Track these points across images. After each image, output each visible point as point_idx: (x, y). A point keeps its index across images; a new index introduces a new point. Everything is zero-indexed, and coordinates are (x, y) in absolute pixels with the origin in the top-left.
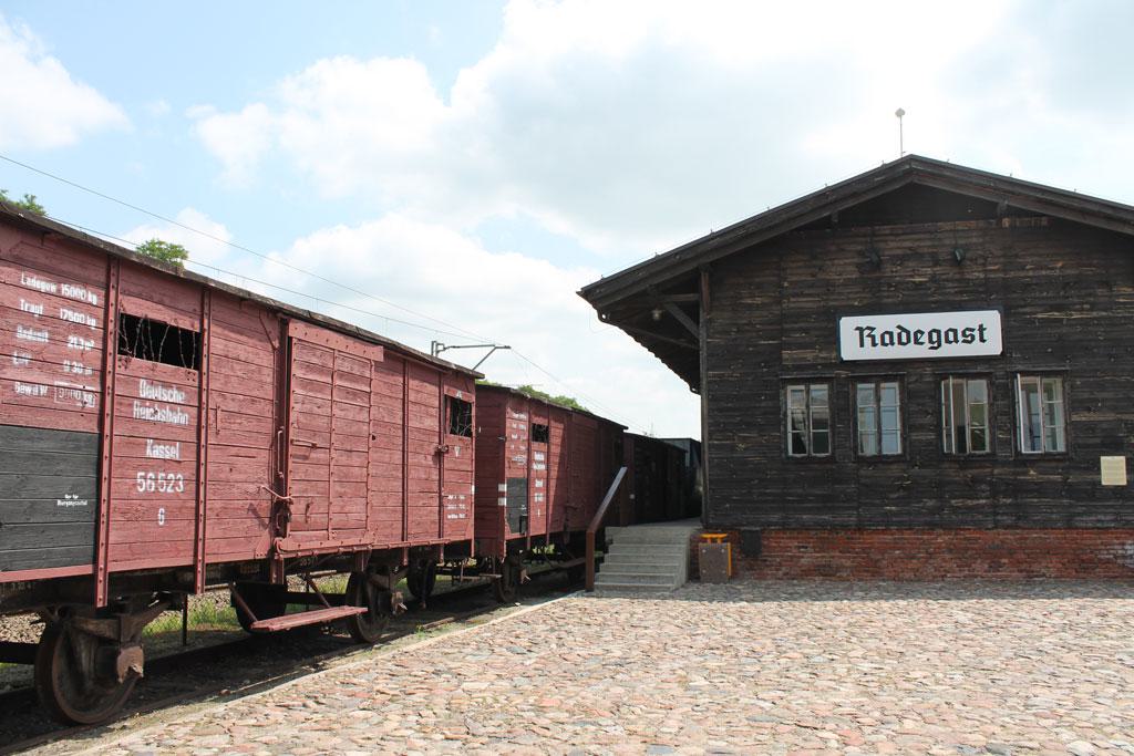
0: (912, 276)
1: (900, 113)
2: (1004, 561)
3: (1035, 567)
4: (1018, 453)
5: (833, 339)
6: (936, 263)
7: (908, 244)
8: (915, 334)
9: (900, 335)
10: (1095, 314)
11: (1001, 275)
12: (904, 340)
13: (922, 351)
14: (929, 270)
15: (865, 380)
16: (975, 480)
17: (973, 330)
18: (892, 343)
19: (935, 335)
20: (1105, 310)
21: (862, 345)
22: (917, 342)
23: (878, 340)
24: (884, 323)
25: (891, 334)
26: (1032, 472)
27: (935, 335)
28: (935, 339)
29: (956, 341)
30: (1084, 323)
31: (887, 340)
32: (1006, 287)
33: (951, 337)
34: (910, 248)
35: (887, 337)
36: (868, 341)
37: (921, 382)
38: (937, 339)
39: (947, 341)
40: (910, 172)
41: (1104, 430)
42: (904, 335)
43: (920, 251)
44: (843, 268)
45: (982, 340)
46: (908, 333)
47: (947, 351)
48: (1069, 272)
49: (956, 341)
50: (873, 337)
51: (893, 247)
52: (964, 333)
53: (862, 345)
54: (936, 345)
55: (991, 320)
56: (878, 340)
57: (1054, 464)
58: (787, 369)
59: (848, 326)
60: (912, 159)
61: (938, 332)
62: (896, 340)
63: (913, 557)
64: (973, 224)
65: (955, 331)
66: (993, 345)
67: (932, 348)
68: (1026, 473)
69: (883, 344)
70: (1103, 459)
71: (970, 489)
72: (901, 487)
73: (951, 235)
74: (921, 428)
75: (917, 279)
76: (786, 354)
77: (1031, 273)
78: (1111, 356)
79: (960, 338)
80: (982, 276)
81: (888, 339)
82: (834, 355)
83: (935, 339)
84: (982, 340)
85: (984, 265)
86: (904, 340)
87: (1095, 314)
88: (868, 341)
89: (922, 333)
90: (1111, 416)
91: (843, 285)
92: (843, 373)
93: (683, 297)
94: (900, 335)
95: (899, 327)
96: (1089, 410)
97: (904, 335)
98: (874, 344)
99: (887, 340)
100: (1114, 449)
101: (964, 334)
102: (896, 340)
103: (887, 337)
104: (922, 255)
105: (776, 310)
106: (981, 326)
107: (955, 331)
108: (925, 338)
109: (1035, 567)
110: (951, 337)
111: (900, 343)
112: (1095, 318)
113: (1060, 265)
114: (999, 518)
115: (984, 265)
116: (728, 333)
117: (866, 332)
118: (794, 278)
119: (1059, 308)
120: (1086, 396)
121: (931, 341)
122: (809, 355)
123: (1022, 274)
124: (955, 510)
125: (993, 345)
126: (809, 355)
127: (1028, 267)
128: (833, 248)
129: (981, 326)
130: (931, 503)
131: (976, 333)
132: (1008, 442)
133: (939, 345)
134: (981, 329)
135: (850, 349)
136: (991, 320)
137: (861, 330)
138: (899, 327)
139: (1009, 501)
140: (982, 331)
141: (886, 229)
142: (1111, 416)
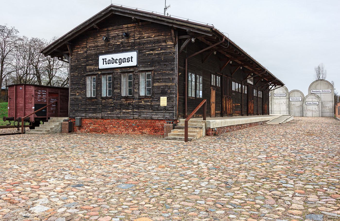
0: (117, 42)
2: (136, 129)
3: (144, 131)
4: (139, 96)
5: (97, 64)
6: (123, 38)
7: (117, 32)
8: (116, 60)
9: (112, 60)
10: (161, 51)
11: (138, 40)
12: (113, 62)
14: (121, 40)
15: (104, 74)
16: (129, 104)
17: (129, 58)
18: (110, 63)
19: (120, 60)
20: (164, 50)
21: (103, 64)
22: (116, 63)
23: (107, 63)
24: (108, 57)
25: (110, 60)
26: (143, 102)
27: (120, 60)
28: (120, 61)
29: (125, 62)
30: (158, 54)
31: (109, 63)
32: (139, 44)
33: (124, 59)
34: (116, 34)
36: (105, 62)
37: (114, 74)
38: (121, 61)
39: (123, 62)
40: (112, 10)
41: (162, 89)
42: (113, 60)
43: (119, 34)
44: (101, 41)
45: (132, 61)
46: (114, 60)
47: (124, 65)
48: (156, 38)
49: (125, 62)
50: (106, 61)
51: (113, 34)
52: (127, 59)
53: (103, 64)
54: (120, 63)
55: (134, 54)
56: (107, 63)
57: (149, 99)
58: (87, 72)
59: (101, 58)
60: (111, 6)
61: (121, 59)
62: (111, 62)
63: (115, 127)
64: (132, 25)
66: (134, 63)
67: (119, 64)
68: (141, 102)
69: (108, 64)
70: (161, 97)
71: (127, 107)
72: (111, 106)
73: (126, 29)
74: (117, 88)
75: (118, 43)
76: (87, 67)
77: (146, 39)
78: (165, 65)
79: (126, 61)
80: (133, 41)
82: (98, 67)
83: (120, 61)
85: (134, 38)
86: (113, 62)
87: (161, 51)
88: (105, 62)
89: (117, 60)
90: (164, 84)
91: (101, 46)
92: (100, 73)
94: (112, 60)
95: (112, 58)
96: (158, 82)
97: (113, 60)
98: (106, 64)
100: (164, 93)
101: (127, 60)
102: (111, 62)
104: (119, 36)
105: (85, 55)
106: (132, 57)
107: (125, 59)
108: (118, 61)
109: (144, 131)
110: (124, 59)
111: (112, 63)
112: (161, 53)
113: (153, 36)
114: (134, 116)
115: (134, 38)
116: (75, 62)
118: (90, 45)
119: (152, 50)
120: (158, 78)
122: (92, 67)
123: (143, 40)
124: (124, 113)
125: (134, 63)
126: (92, 67)
127: (145, 37)
128: (99, 35)
129: (132, 57)
130: (118, 111)
131: (130, 59)
132: (137, 93)
133: (121, 63)
134: (132, 58)
135: (101, 66)
136: (134, 54)
137: (103, 59)
138: (112, 58)
139: (137, 110)
140: (131, 58)
141: (110, 28)
142: (164, 84)
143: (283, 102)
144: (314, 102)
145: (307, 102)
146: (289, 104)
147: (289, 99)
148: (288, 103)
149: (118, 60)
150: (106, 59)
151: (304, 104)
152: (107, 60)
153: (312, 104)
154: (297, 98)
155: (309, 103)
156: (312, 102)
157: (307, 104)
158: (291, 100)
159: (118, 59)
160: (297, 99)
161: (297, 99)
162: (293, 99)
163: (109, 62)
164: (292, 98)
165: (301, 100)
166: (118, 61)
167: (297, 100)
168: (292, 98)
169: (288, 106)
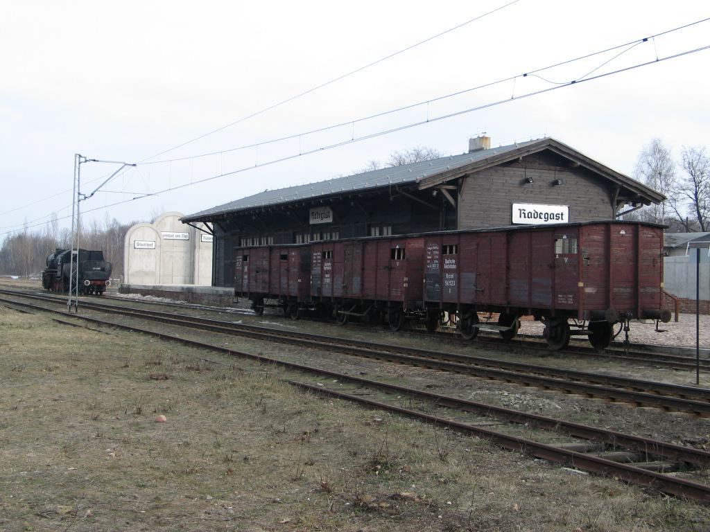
22: (540, 218)
23: (526, 216)
24: (530, 207)
36: (523, 215)
38: (548, 216)
46: (537, 213)
47: (551, 222)
50: (525, 214)
56: (526, 216)
59: (516, 207)
65: (553, 214)
69: (528, 217)
79: (555, 217)
81: (530, 215)
93: (451, 187)
98: (525, 217)
108: (543, 216)
117: (522, 211)
131: (560, 216)
134: (562, 214)
152: (526, 212)
163: (530, 215)
166: (543, 216)
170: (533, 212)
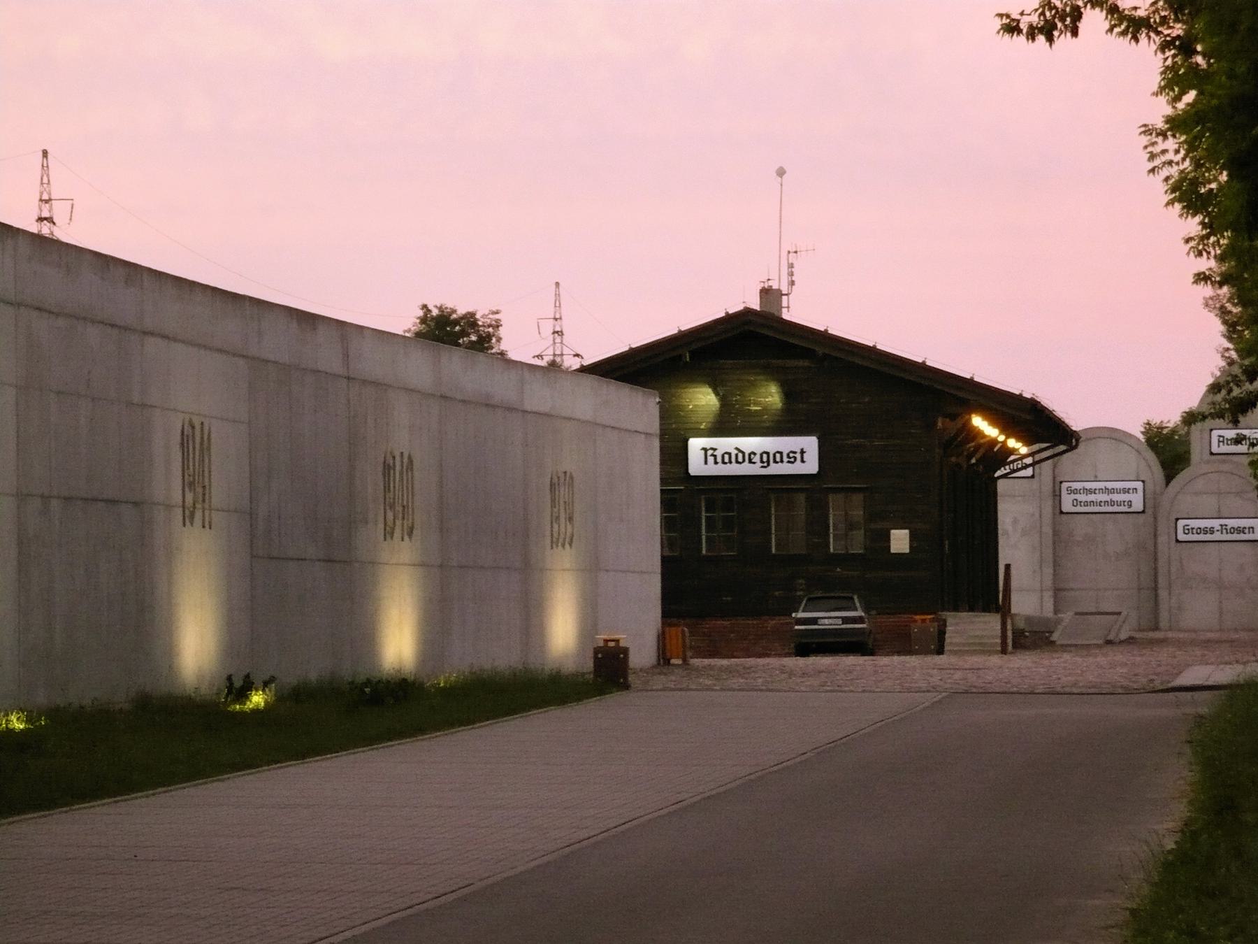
1: (781, 172)
12: (740, 459)
13: (755, 470)
19: (765, 456)
21: (706, 463)
22: (750, 462)
23: (719, 459)
25: (730, 454)
27: (765, 456)
29: (782, 461)
31: (727, 460)
33: (778, 456)
35: (727, 457)
36: (711, 459)
39: (775, 462)
42: (740, 455)
45: (803, 461)
46: (743, 453)
49: (782, 461)
50: (715, 456)
53: (706, 463)
55: (810, 444)
56: (719, 459)
61: (768, 453)
66: (811, 466)
69: (724, 463)
79: (785, 459)
81: (727, 458)
84: (803, 461)
86: (740, 459)
88: (711, 459)
97: (740, 455)
98: (716, 463)
99: (727, 460)
103: (727, 457)
107: (781, 453)
108: (757, 459)
110: (778, 459)
111: (737, 462)
117: (710, 452)
121: (762, 462)
125: (811, 466)
134: (802, 452)
136: (810, 444)
137: (705, 450)
143: (1015, 521)
144: (1232, 523)
145: (1181, 523)
146: (1056, 533)
147: (1057, 495)
148: (1048, 530)
149: (758, 457)
150: (715, 450)
151: (1162, 539)
152: (719, 453)
153: (1217, 536)
154: (1112, 491)
155: (1200, 531)
156: (1216, 523)
157: (1181, 537)
158: (1067, 506)
159: (758, 453)
160: (1116, 497)
161: (1116, 497)
162: (1082, 497)
164: (1075, 491)
165: (1138, 505)
166: (757, 459)
167: (1112, 503)
168: (1075, 491)
169: (1048, 552)
170: (734, 452)
